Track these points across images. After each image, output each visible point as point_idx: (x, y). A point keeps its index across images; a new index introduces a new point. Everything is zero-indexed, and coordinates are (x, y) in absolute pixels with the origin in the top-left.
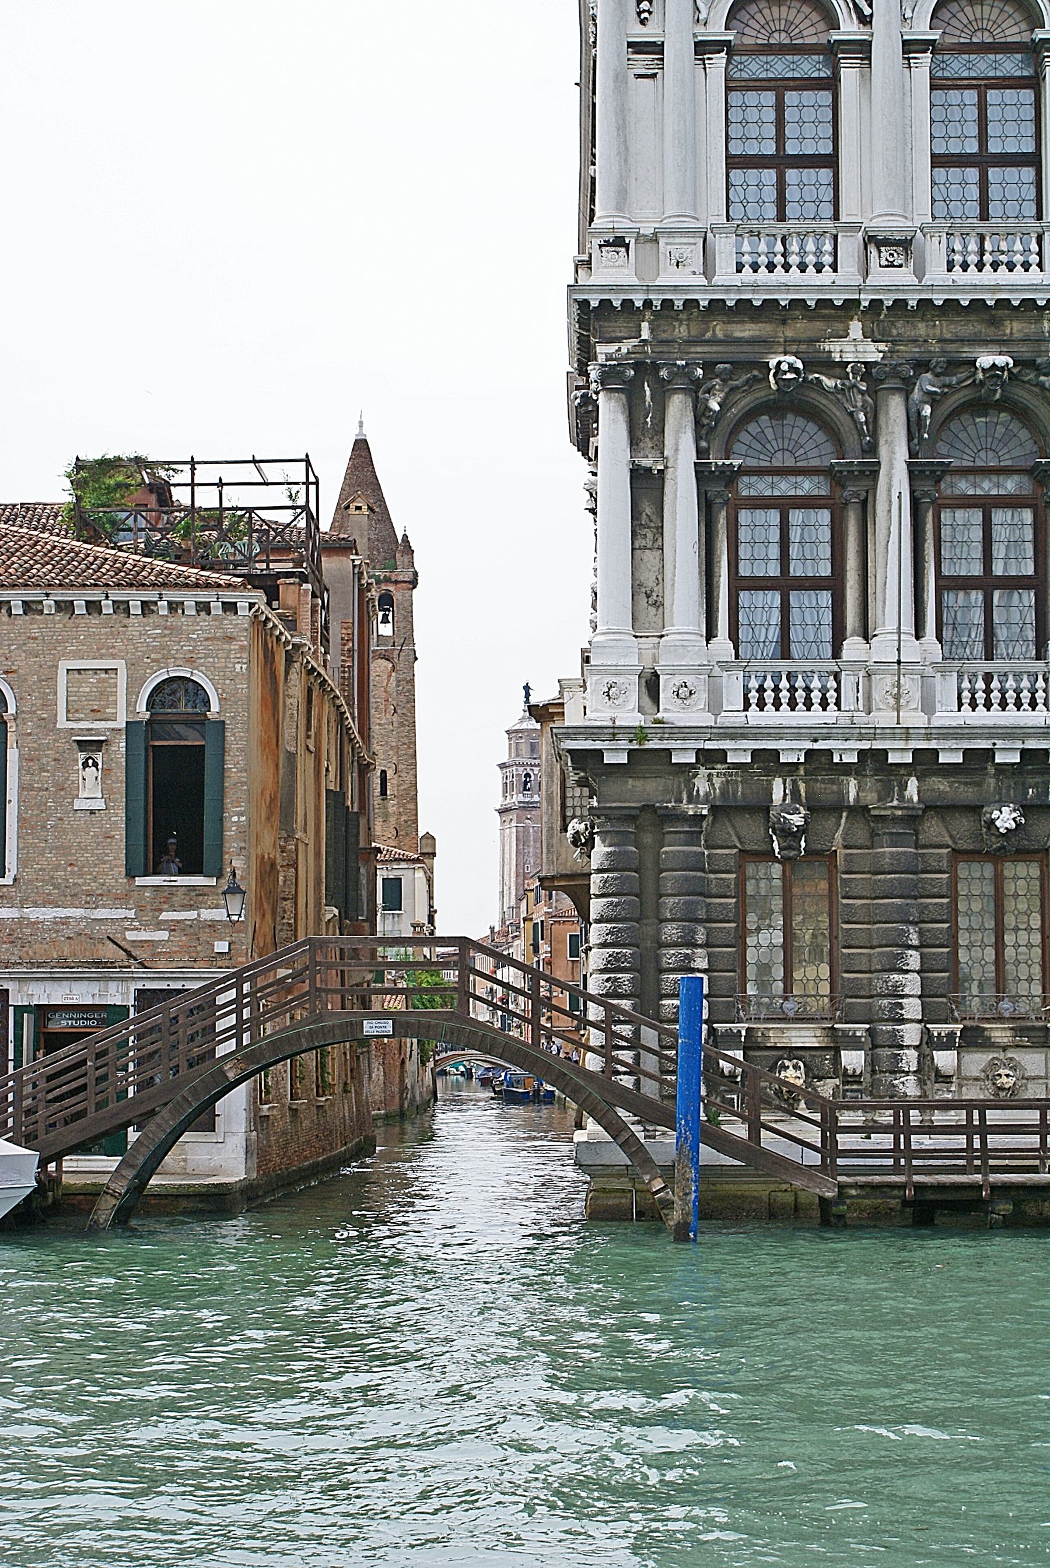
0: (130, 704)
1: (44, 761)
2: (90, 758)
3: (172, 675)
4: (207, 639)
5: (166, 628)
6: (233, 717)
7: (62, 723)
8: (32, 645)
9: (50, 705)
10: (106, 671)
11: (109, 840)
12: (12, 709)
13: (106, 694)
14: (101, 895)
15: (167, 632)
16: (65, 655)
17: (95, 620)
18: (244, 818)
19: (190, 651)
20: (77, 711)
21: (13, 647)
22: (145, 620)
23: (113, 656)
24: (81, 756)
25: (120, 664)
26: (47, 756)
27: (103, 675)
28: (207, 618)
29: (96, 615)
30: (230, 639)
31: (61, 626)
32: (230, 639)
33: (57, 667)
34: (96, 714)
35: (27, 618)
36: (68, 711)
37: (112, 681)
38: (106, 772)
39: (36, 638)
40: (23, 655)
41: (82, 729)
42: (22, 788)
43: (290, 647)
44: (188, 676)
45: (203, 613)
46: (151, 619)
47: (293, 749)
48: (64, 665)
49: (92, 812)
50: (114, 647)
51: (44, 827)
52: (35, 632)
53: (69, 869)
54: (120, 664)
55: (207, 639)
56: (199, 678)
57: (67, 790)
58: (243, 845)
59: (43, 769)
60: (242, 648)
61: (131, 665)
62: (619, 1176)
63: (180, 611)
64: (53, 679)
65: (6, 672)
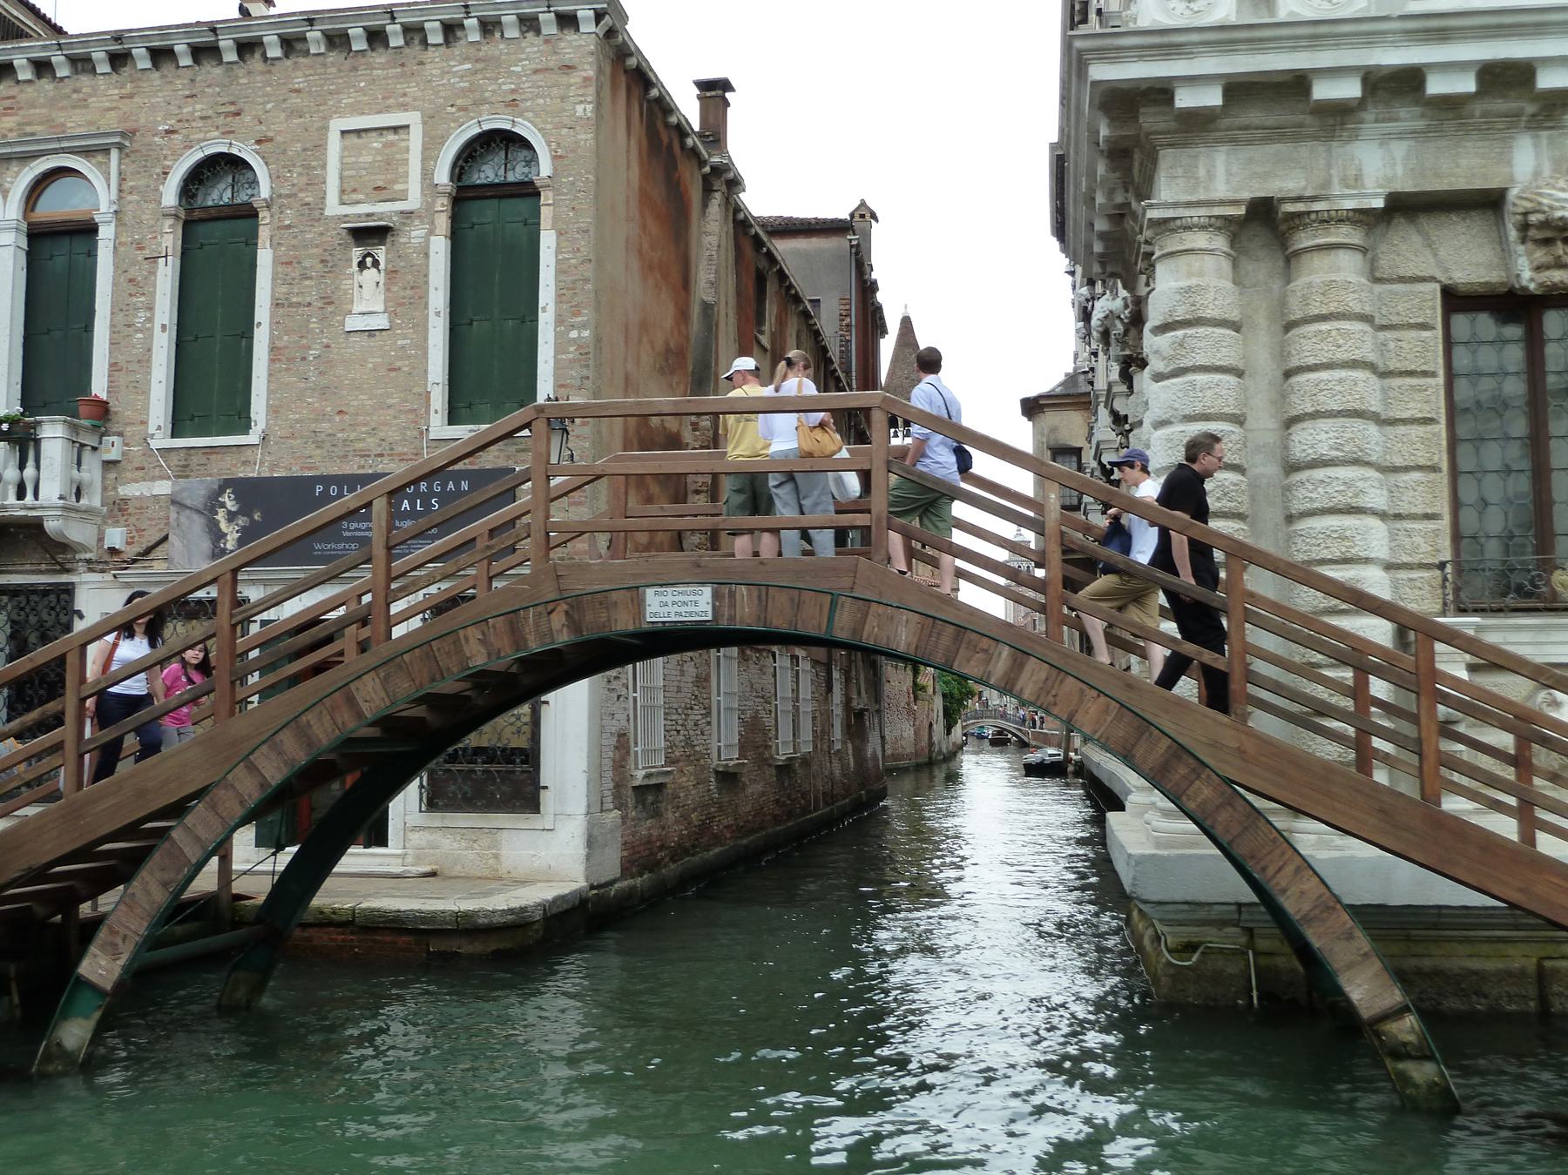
0: (427, 174)
1: (306, 264)
2: (369, 255)
3: (486, 127)
4: (536, 71)
5: (477, 61)
6: (573, 183)
7: (333, 207)
8: (295, 100)
9: (316, 183)
10: (395, 129)
11: (393, 374)
12: (265, 191)
13: (393, 164)
14: (381, 455)
15: (479, 66)
16: (339, 112)
17: (380, 57)
18: (586, 333)
19: (513, 91)
20: (354, 190)
21: (269, 106)
22: (448, 51)
23: (404, 107)
24: (356, 253)
25: (413, 118)
26: (310, 256)
27: (391, 137)
28: (536, 40)
29: (381, 50)
30: (568, 68)
31: (334, 70)
32: (568, 68)
33: (326, 128)
34: (381, 192)
35: (288, 63)
36: (343, 192)
37: (403, 144)
38: (392, 274)
39: (298, 91)
40: (283, 116)
41: (360, 216)
42: (276, 304)
43: (707, 169)
44: (507, 126)
45: (530, 35)
46: (458, 49)
47: (710, 299)
48: (337, 125)
49: (371, 333)
50: (405, 95)
51: (304, 359)
52: (299, 82)
53: (337, 418)
54: (413, 118)
55: (536, 71)
56: (524, 129)
57: (334, 304)
58: (585, 372)
59: (305, 277)
60: (586, 79)
61: (428, 119)
62: (1222, 923)
63: (498, 35)
64: (320, 147)
65: (259, 142)
